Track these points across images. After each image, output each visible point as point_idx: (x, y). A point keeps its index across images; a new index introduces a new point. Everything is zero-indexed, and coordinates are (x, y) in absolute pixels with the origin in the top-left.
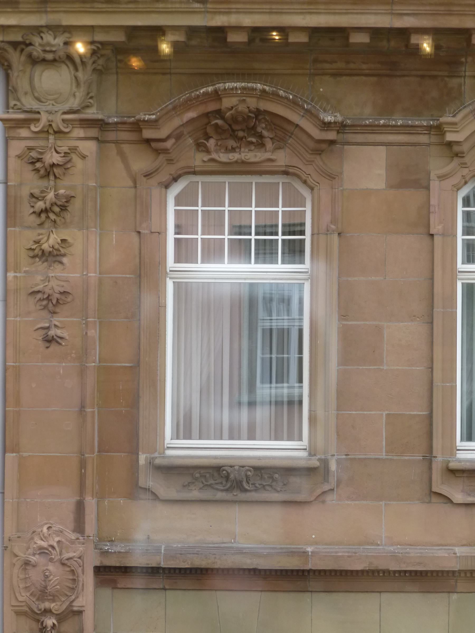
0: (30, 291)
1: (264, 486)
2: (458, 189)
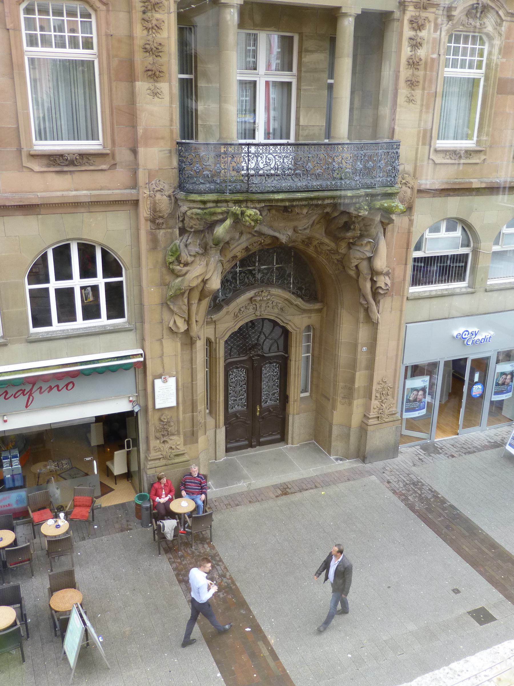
2: (20, 4)
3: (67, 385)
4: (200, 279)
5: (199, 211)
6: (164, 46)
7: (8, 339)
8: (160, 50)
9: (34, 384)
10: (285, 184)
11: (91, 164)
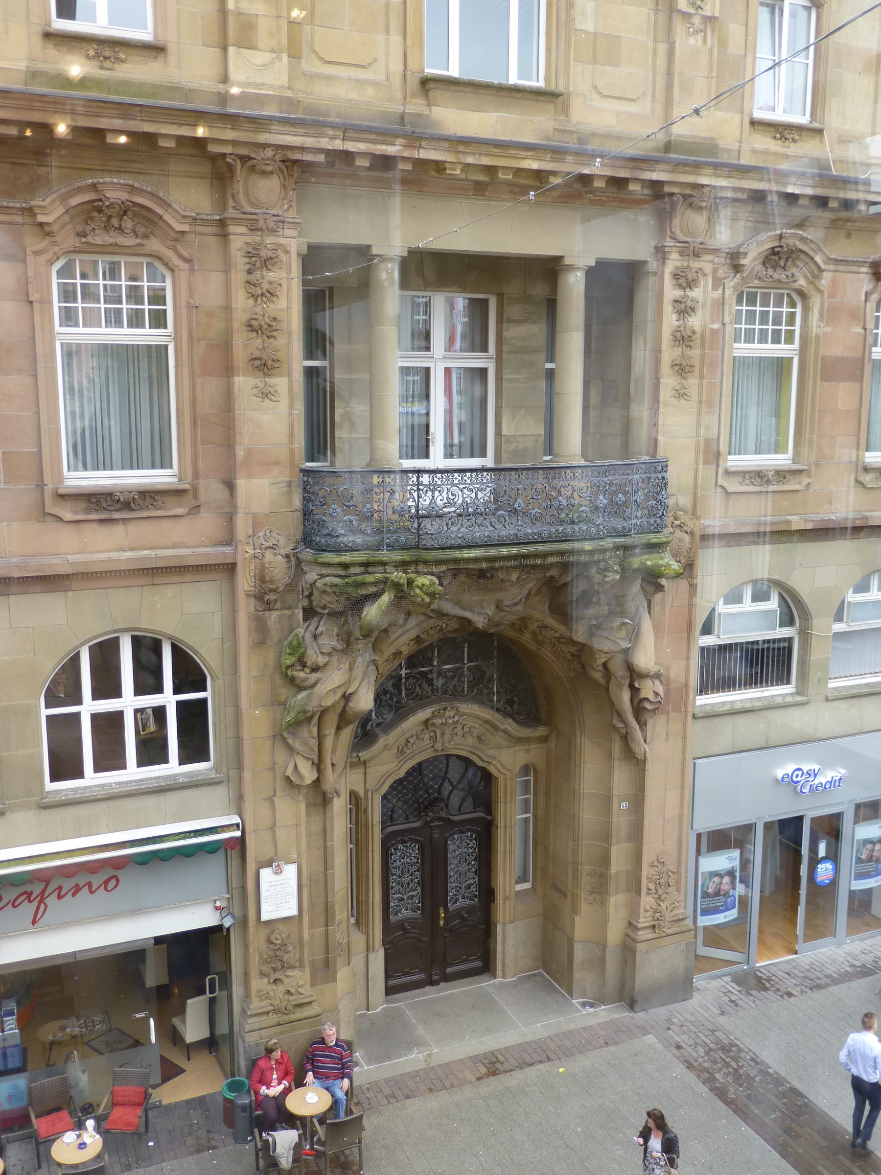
2: (52, 264)
3: (106, 883)
4: (339, 694)
7: (7, 802)
8: (274, 328)
10: (478, 534)
11: (158, 507)
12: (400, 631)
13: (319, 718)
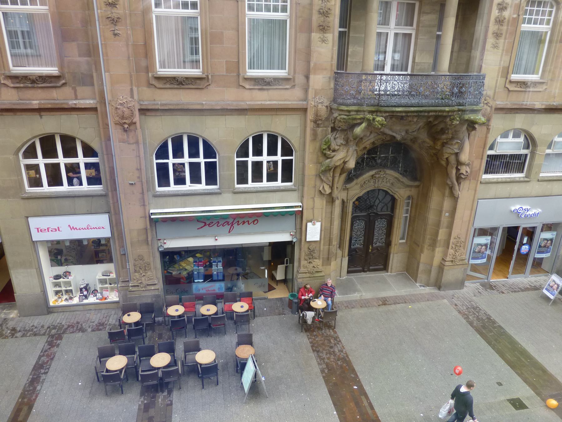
0: (107, 17)
1: (189, 84)
3: (254, 222)
4: (342, 161)
5: (345, 117)
6: (331, 10)
7: (222, 190)
8: (329, 13)
9: (234, 219)
10: (403, 101)
12: (367, 139)
13: (334, 170)
